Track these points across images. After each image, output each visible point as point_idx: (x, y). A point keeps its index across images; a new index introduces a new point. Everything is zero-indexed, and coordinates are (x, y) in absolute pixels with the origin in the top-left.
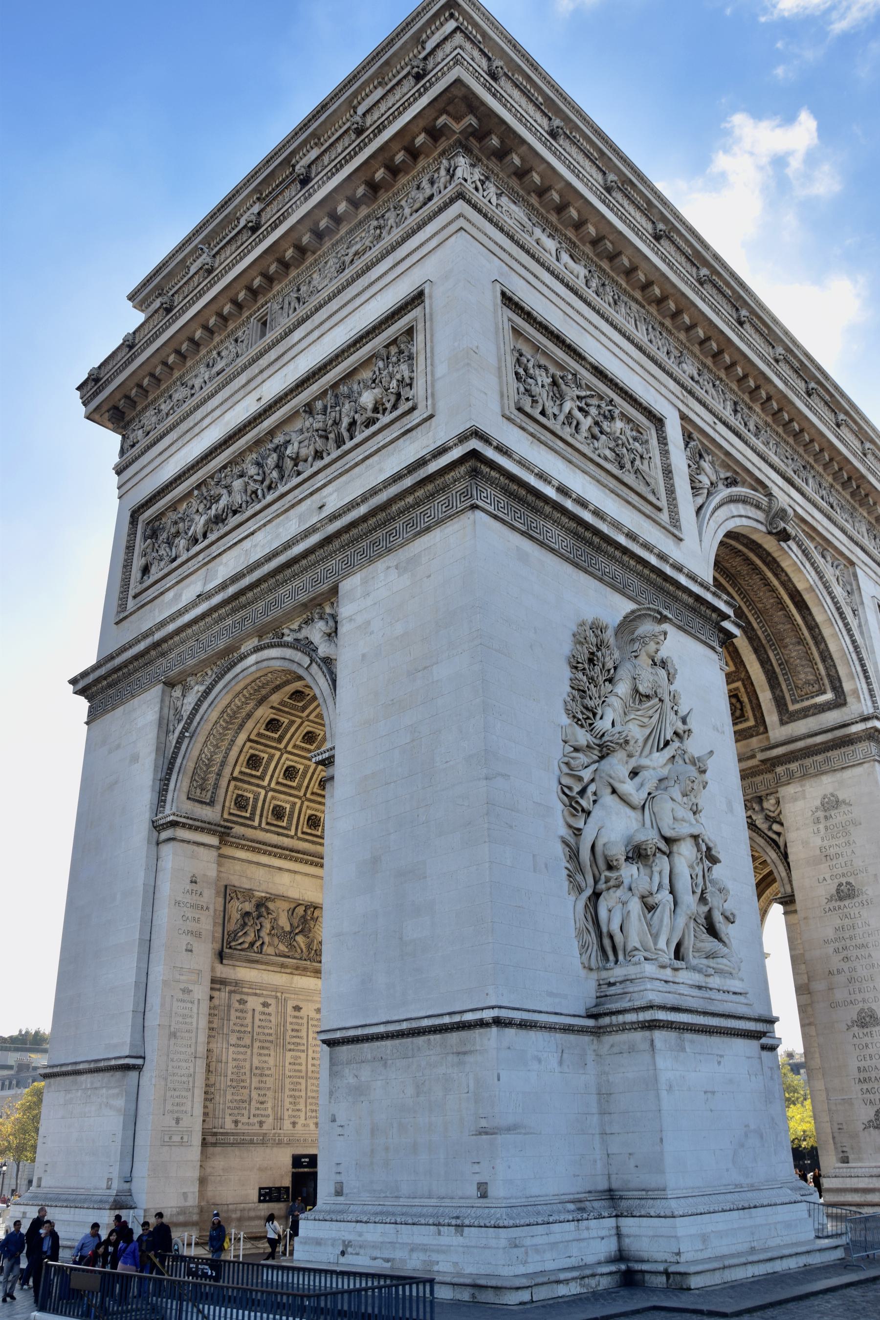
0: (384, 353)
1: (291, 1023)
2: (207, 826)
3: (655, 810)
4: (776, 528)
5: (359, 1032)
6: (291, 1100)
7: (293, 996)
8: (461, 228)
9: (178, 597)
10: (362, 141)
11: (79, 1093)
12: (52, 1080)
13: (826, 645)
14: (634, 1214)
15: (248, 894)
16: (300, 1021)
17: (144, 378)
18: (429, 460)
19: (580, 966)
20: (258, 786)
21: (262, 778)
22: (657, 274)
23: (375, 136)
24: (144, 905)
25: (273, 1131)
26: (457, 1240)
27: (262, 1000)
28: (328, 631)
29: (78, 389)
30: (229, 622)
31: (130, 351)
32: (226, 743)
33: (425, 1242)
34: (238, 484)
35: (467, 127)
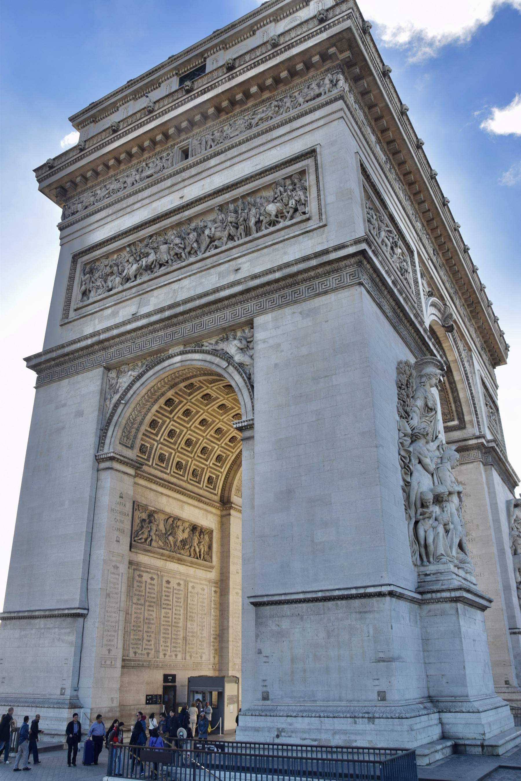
0: (282, 182)
1: (165, 591)
2: (131, 462)
3: (440, 475)
4: (448, 324)
5: (283, 598)
6: (164, 640)
7: (166, 574)
8: (342, 117)
9: (115, 314)
10: (276, 52)
11: (34, 631)
12: (8, 622)
13: (458, 394)
14: (451, 710)
15: (145, 508)
16: (169, 590)
17: (88, 171)
18: (332, 251)
19: (412, 563)
20: (154, 440)
21: (156, 435)
22: (415, 167)
23: (285, 50)
24: (89, 510)
25: (154, 659)
26: (370, 727)
27: (150, 576)
28: (242, 347)
29: (34, 171)
30: (161, 333)
31: (80, 152)
32: (145, 410)
33: (344, 728)
34: (164, 248)
35: (346, 58)
